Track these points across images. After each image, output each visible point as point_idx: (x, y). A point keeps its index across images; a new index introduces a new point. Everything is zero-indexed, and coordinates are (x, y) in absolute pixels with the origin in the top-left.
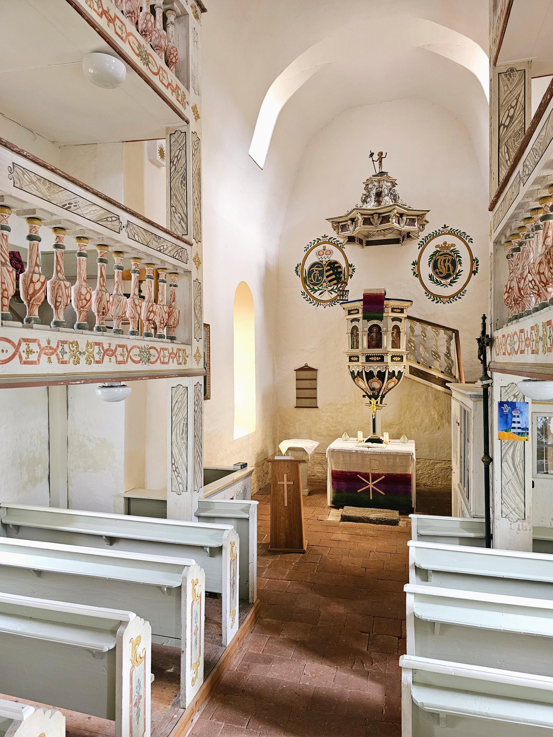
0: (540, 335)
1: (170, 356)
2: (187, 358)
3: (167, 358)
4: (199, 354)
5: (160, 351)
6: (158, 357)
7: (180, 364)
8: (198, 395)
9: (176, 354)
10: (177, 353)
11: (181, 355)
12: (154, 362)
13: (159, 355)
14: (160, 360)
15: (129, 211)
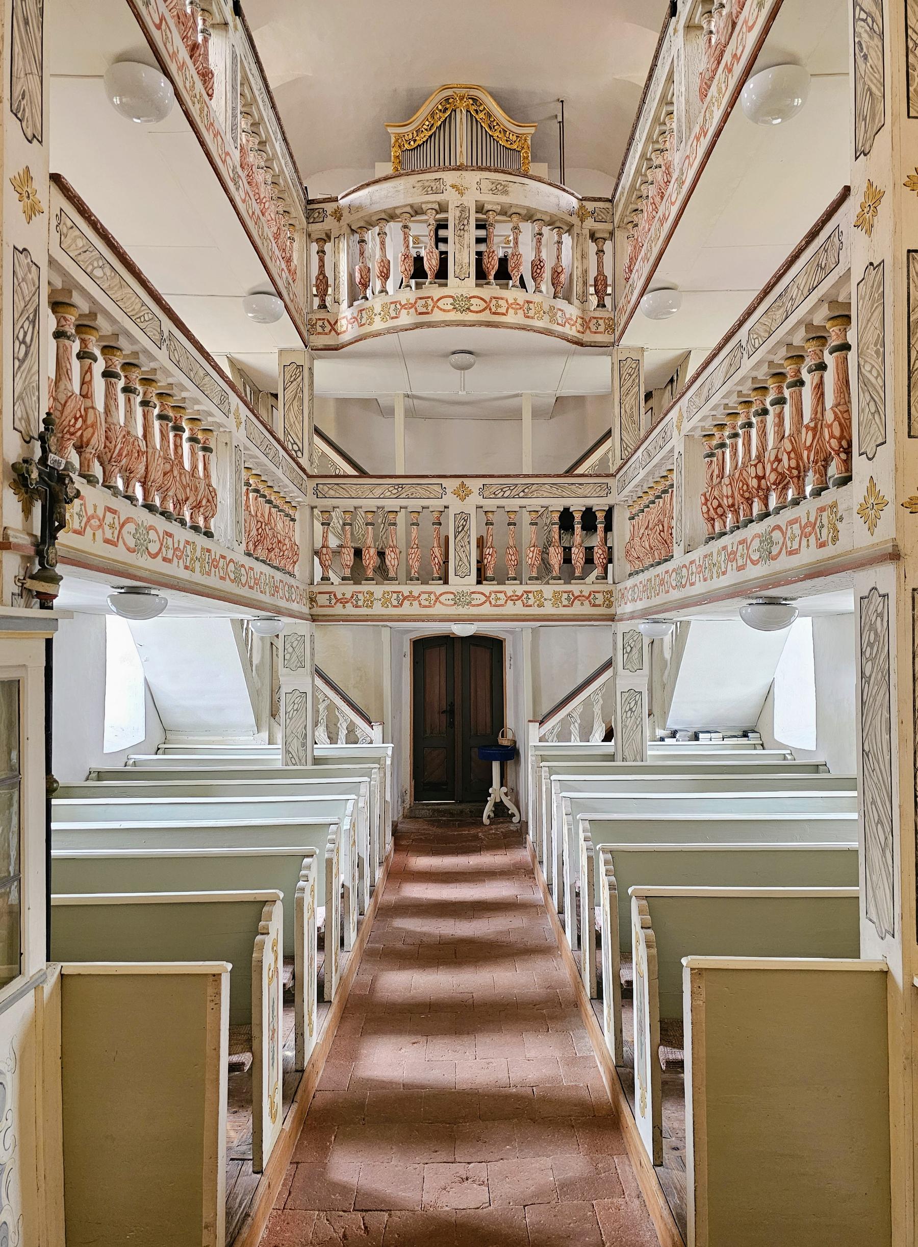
0: (196, 555)
1: (802, 533)
2: (840, 526)
3: (797, 539)
4: (877, 497)
5: (787, 529)
6: (783, 543)
7: (822, 545)
8: (873, 628)
9: (815, 524)
10: (816, 519)
11: (825, 521)
12: (776, 555)
13: (785, 538)
14: (786, 548)
15: (744, 317)
